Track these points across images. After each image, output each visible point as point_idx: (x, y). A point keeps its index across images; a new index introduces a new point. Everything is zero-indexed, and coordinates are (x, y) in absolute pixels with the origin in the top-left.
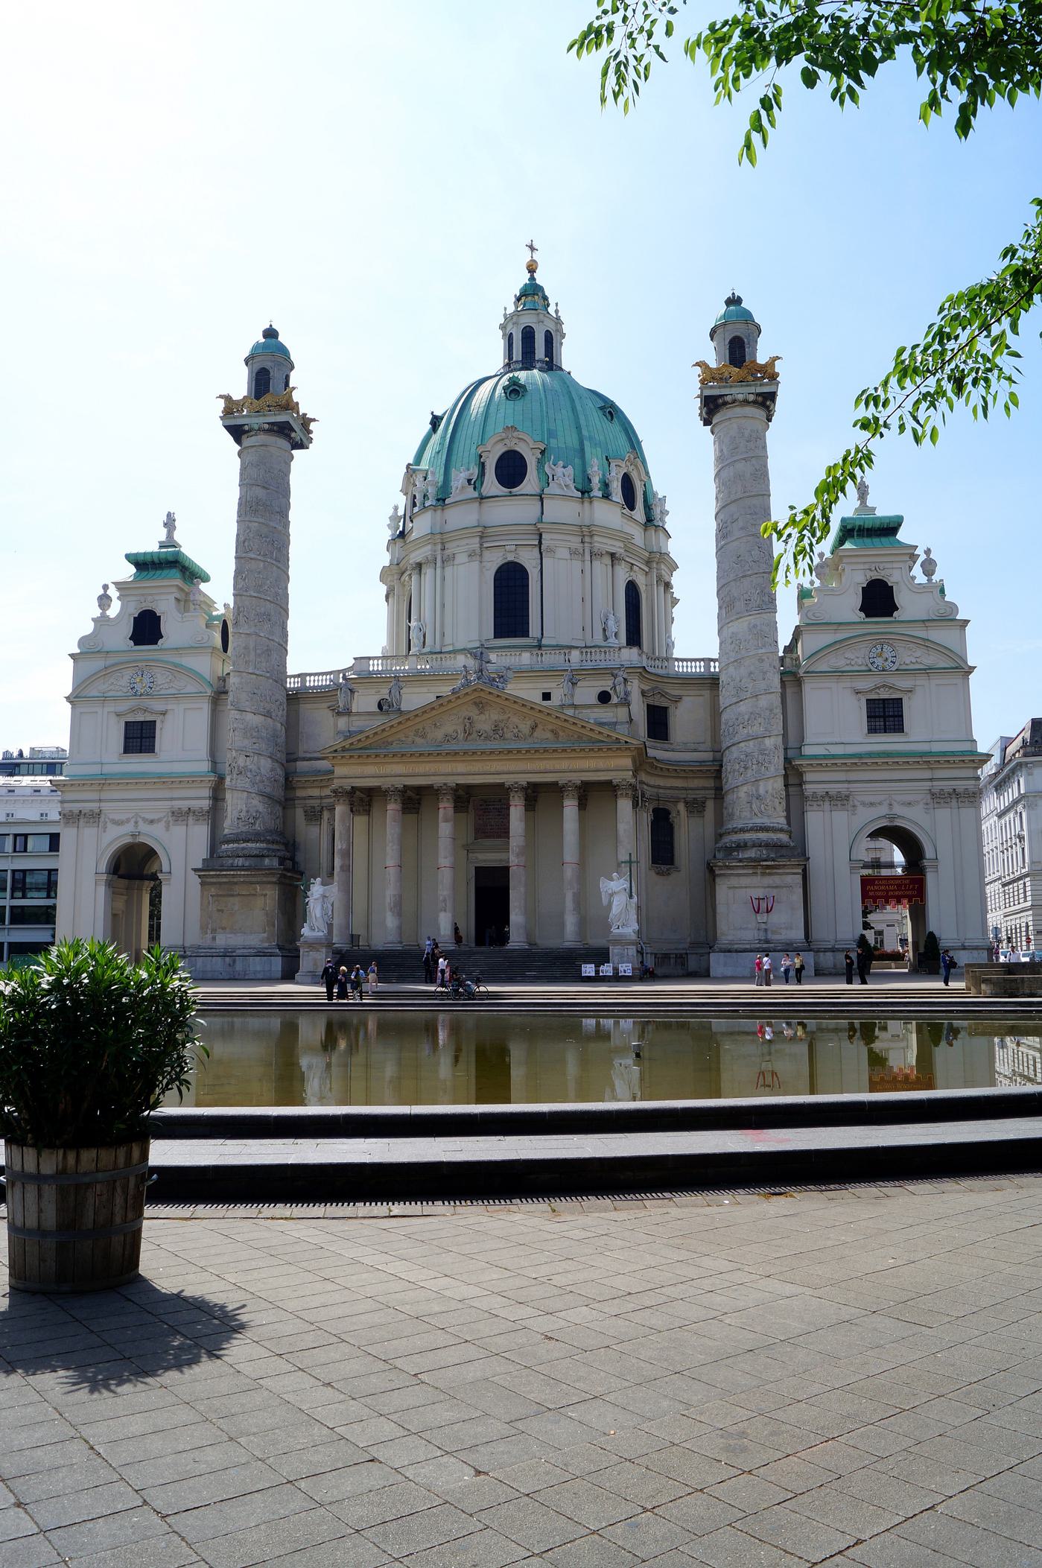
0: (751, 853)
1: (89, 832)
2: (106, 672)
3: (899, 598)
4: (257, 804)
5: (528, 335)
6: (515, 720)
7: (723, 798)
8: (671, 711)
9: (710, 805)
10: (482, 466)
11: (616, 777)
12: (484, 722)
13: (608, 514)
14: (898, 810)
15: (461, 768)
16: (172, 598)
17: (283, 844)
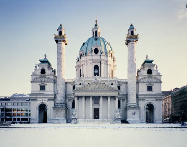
0: (132, 107)
1: (34, 102)
2: (37, 78)
3: (153, 72)
4: (62, 99)
5: (96, 32)
6: (101, 87)
7: (127, 99)
8: (120, 87)
9: (125, 100)
10: (92, 50)
11: (116, 95)
12: (97, 87)
13: (109, 58)
14: (151, 101)
15: (93, 93)
16: (47, 67)
17: (65, 104)
